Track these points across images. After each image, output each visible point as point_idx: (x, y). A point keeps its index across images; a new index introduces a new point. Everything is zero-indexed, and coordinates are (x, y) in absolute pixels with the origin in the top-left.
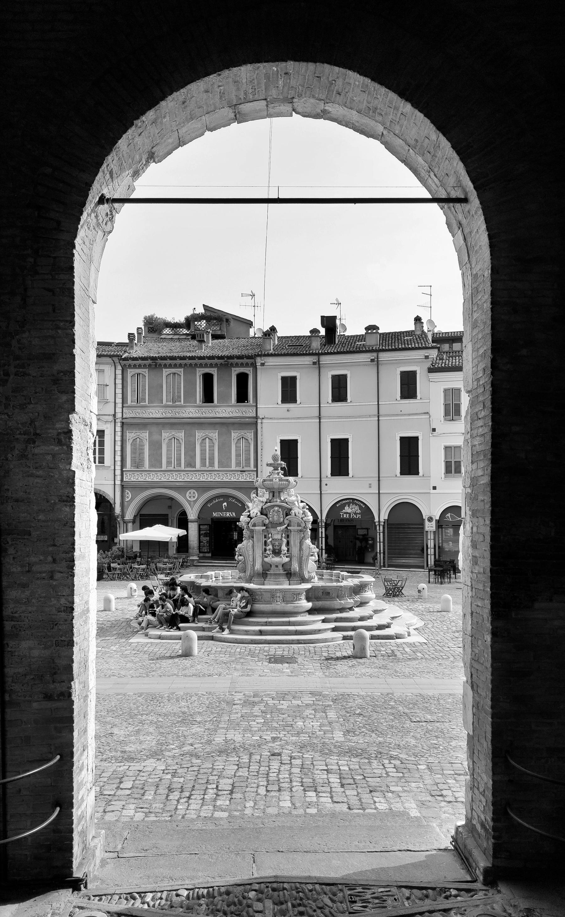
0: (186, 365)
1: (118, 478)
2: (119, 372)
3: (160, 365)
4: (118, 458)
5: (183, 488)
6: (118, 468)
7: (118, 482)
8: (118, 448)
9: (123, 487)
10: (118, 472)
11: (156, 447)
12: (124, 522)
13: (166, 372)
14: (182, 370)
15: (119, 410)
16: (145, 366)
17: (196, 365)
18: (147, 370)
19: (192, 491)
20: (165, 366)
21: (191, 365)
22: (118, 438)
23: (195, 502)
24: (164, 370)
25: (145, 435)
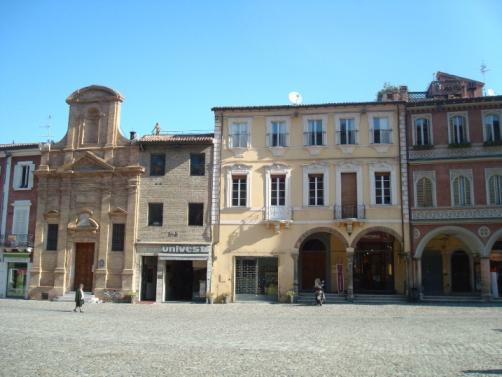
0: (470, 107)
1: (407, 216)
2: (402, 118)
3: (443, 109)
4: (405, 198)
5: (473, 227)
6: (406, 206)
7: (406, 221)
8: (405, 188)
9: (411, 227)
10: (406, 211)
11: (444, 186)
12: (413, 259)
13: (450, 115)
14: (466, 112)
15: (403, 153)
16: (428, 111)
17: (480, 106)
18: (430, 115)
19: (484, 228)
20: (449, 110)
21: (475, 107)
22: (404, 179)
23: (488, 238)
24: (449, 114)
25: (432, 175)
